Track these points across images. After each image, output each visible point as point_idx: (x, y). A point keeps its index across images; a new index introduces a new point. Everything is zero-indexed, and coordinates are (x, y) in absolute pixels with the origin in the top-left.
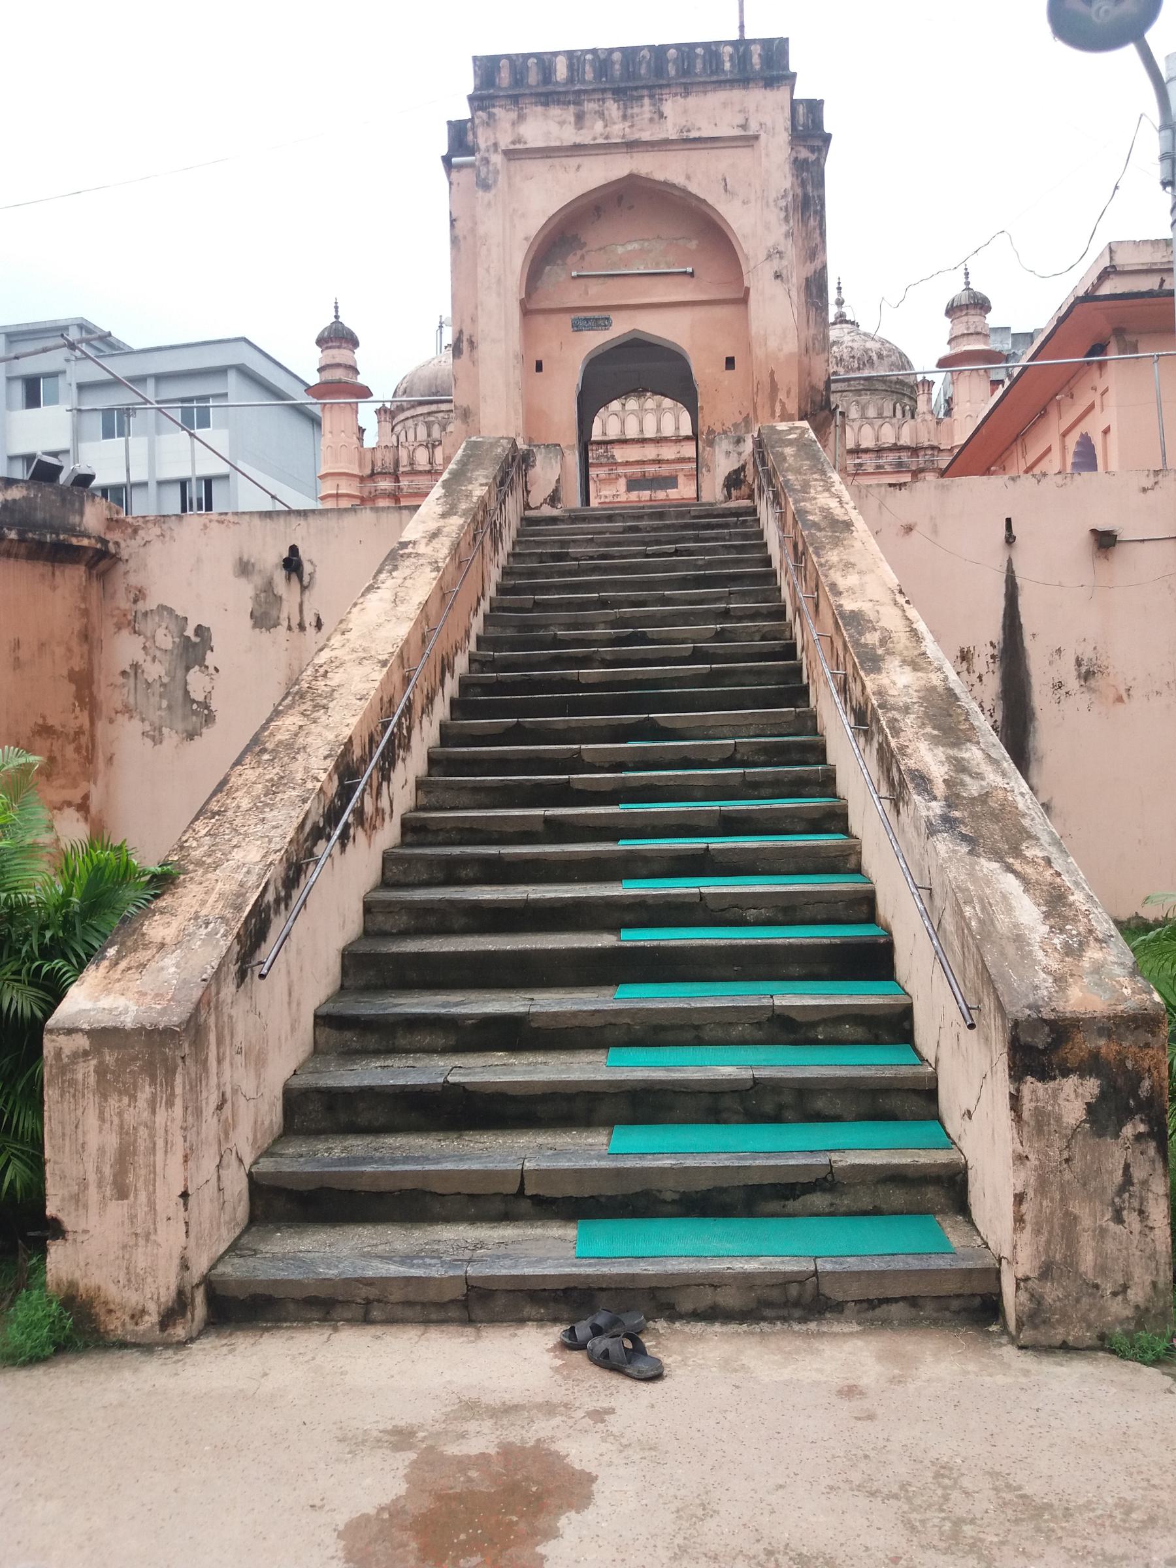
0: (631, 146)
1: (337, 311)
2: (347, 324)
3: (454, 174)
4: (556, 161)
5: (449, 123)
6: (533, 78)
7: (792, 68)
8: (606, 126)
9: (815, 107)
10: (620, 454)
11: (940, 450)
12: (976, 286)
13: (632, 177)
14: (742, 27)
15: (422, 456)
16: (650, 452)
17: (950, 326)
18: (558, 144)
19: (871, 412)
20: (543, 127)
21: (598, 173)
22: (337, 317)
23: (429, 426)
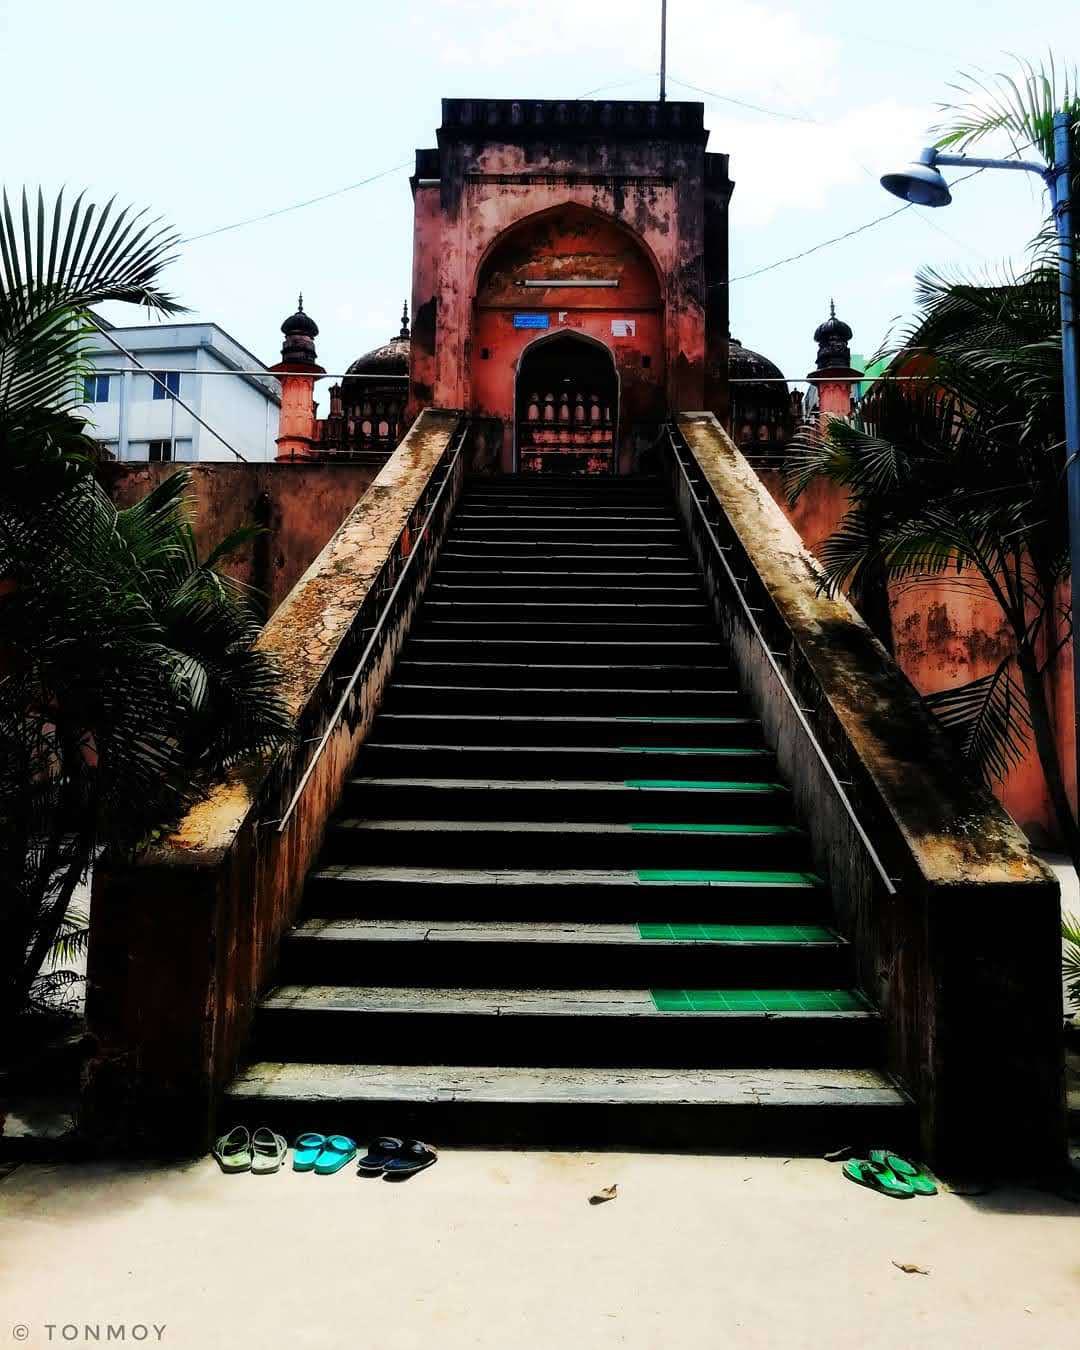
0: (572, 179)
2: (309, 316)
3: (419, 194)
4: (509, 187)
5: (417, 151)
6: (493, 119)
7: (706, 127)
8: (551, 162)
9: (721, 161)
10: (536, 436)
12: (840, 318)
13: (570, 205)
14: (663, 95)
16: (564, 437)
17: (818, 348)
18: (511, 173)
20: (500, 159)
21: (543, 198)
22: (301, 308)
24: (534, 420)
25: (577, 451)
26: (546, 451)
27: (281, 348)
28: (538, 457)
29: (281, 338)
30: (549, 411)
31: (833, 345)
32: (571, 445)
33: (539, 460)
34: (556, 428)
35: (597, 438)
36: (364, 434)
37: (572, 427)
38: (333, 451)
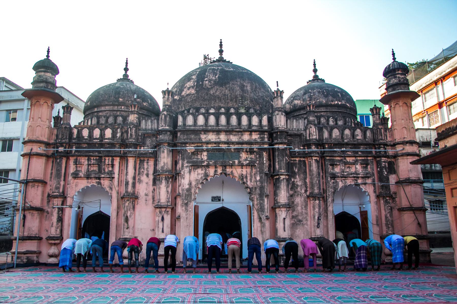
1: (48, 53)
10: (204, 137)
11: (386, 145)
15: (85, 133)
16: (223, 137)
19: (340, 123)
22: (48, 56)
23: (98, 118)
24: (202, 126)
25: (232, 147)
26: (210, 146)
27: (32, 81)
28: (204, 151)
29: (33, 74)
30: (212, 120)
31: (399, 77)
32: (227, 143)
33: (205, 153)
34: (218, 132)
35: (246, 137)
36: (83, 137)
37: (229, 132)
38: (61, 149)
